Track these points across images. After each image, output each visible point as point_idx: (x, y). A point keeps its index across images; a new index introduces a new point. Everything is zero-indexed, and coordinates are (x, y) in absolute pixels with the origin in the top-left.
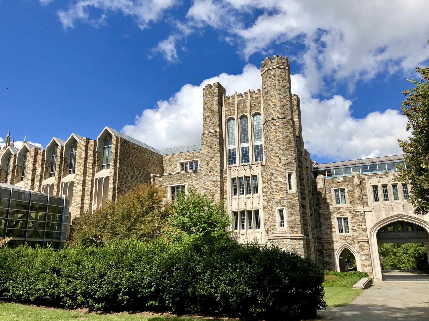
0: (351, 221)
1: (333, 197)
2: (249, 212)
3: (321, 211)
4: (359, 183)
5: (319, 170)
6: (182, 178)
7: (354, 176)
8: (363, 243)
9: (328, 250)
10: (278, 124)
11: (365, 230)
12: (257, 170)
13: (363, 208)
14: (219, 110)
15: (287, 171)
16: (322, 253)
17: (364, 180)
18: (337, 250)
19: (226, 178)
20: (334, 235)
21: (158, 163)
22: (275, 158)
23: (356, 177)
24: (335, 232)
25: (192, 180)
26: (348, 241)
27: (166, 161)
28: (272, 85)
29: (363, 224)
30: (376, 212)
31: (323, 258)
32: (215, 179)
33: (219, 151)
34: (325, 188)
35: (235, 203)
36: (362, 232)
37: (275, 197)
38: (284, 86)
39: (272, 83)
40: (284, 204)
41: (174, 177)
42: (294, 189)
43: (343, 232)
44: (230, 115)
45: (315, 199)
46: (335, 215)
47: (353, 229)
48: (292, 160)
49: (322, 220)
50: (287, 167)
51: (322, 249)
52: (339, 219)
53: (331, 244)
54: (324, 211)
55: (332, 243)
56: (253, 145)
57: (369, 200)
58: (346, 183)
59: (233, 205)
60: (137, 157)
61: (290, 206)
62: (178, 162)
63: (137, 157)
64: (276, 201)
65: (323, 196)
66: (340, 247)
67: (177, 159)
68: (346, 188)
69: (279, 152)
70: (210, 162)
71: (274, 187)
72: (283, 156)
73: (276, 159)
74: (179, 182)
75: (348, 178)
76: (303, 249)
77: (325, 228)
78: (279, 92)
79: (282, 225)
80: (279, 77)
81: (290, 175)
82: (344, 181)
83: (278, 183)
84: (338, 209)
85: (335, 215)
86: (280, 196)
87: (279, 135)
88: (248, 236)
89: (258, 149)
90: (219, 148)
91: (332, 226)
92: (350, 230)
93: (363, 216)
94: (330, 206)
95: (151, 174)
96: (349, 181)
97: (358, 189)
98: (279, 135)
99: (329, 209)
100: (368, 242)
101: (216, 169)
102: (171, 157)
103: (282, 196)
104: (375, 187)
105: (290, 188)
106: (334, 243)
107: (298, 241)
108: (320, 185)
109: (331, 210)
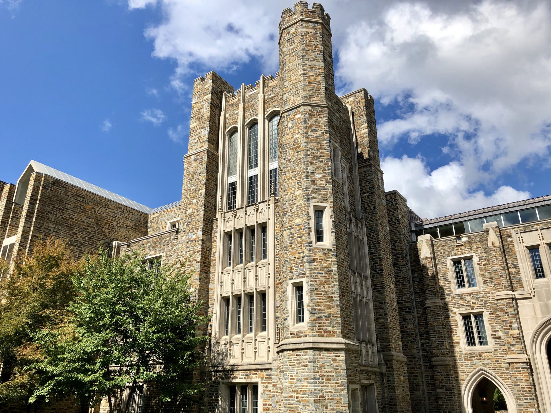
0: (489, 320)
1: (451, 275)
2: (250, 296)
4: (498, 243)
5: (425, 227)
6: (158, 244)
7: (487, 231)
8: (517, 366)
9: (444, 381)
10: (297, 116)
11: (520, 338)
12: (266, 213)
13: (511, 292)
15: (313, 203)
16: (434, 386)
17: (510, 236)
18: (465, 382)
19: (216, 235)
20: (457, 349)
22: (290, 181)
23: (491, 232)
24: (458, 343)
25: (172, 246)
26: (487, 361)
27: (151, 222)
28: (291, 51)
29: (515, 325)
30: (540, 300)
31: (437, 398)
32: (194, 237)
33: (206, 184)
35: (227, 281)
36: (514, 342)
37: (289, 257)
38: (314, 51)
39: (291, 48)
40: (304, 271)
41: (146, 244)
42: (329, 240)
43: (475, 345)
44: (231, 125)
46: (456, 310)
47: (494, 337)
48: (323, 183)
49: (431, 319)
50: (313, 195)
51: (433, 379)
52: (466, 317)
53: (451, 369)
54: (433, 301)
55: (455, 367)
56: (267, 169)
57: (522, 275)
58: (475, 246)
59: (224, 284)
60: (84, 211)
61: (318, 275)
63: (84, 211)
64: (290, 265)
65: (430, 273)
66: (471, 375)
67: (168, 217)
68: (474, 254)
69: (297, 169)
70: (189, 206)
71: (286, 239)
72: (304, 174)
74: (153, 252)
75: (478, 236)
76: (344, 373)
77: (437, 335)
78: (301, 60)
79: (301, 319)
80: (303, 36)
81: (319, 212)
82: (470, 243)
83: (295, 229)
84: (462, 297)
85: (456, 310)
86: (298, 256)
87: (298, 136)
88: (246, 346)
89: (274, 175)
90: (204, 179)
91: (451, 332)
92: (489, 339)
93: (512, 309)
94: (446, 292)
96: (480, 242)
97: (497, 254)
98: (298, 136)
100: (529, 364)
101: (197, 217)
103: (301, 255)
104: (534, 249)
105: (319, 237)
106: (459, 365)
108: (425, 252)
109: (448, 299)
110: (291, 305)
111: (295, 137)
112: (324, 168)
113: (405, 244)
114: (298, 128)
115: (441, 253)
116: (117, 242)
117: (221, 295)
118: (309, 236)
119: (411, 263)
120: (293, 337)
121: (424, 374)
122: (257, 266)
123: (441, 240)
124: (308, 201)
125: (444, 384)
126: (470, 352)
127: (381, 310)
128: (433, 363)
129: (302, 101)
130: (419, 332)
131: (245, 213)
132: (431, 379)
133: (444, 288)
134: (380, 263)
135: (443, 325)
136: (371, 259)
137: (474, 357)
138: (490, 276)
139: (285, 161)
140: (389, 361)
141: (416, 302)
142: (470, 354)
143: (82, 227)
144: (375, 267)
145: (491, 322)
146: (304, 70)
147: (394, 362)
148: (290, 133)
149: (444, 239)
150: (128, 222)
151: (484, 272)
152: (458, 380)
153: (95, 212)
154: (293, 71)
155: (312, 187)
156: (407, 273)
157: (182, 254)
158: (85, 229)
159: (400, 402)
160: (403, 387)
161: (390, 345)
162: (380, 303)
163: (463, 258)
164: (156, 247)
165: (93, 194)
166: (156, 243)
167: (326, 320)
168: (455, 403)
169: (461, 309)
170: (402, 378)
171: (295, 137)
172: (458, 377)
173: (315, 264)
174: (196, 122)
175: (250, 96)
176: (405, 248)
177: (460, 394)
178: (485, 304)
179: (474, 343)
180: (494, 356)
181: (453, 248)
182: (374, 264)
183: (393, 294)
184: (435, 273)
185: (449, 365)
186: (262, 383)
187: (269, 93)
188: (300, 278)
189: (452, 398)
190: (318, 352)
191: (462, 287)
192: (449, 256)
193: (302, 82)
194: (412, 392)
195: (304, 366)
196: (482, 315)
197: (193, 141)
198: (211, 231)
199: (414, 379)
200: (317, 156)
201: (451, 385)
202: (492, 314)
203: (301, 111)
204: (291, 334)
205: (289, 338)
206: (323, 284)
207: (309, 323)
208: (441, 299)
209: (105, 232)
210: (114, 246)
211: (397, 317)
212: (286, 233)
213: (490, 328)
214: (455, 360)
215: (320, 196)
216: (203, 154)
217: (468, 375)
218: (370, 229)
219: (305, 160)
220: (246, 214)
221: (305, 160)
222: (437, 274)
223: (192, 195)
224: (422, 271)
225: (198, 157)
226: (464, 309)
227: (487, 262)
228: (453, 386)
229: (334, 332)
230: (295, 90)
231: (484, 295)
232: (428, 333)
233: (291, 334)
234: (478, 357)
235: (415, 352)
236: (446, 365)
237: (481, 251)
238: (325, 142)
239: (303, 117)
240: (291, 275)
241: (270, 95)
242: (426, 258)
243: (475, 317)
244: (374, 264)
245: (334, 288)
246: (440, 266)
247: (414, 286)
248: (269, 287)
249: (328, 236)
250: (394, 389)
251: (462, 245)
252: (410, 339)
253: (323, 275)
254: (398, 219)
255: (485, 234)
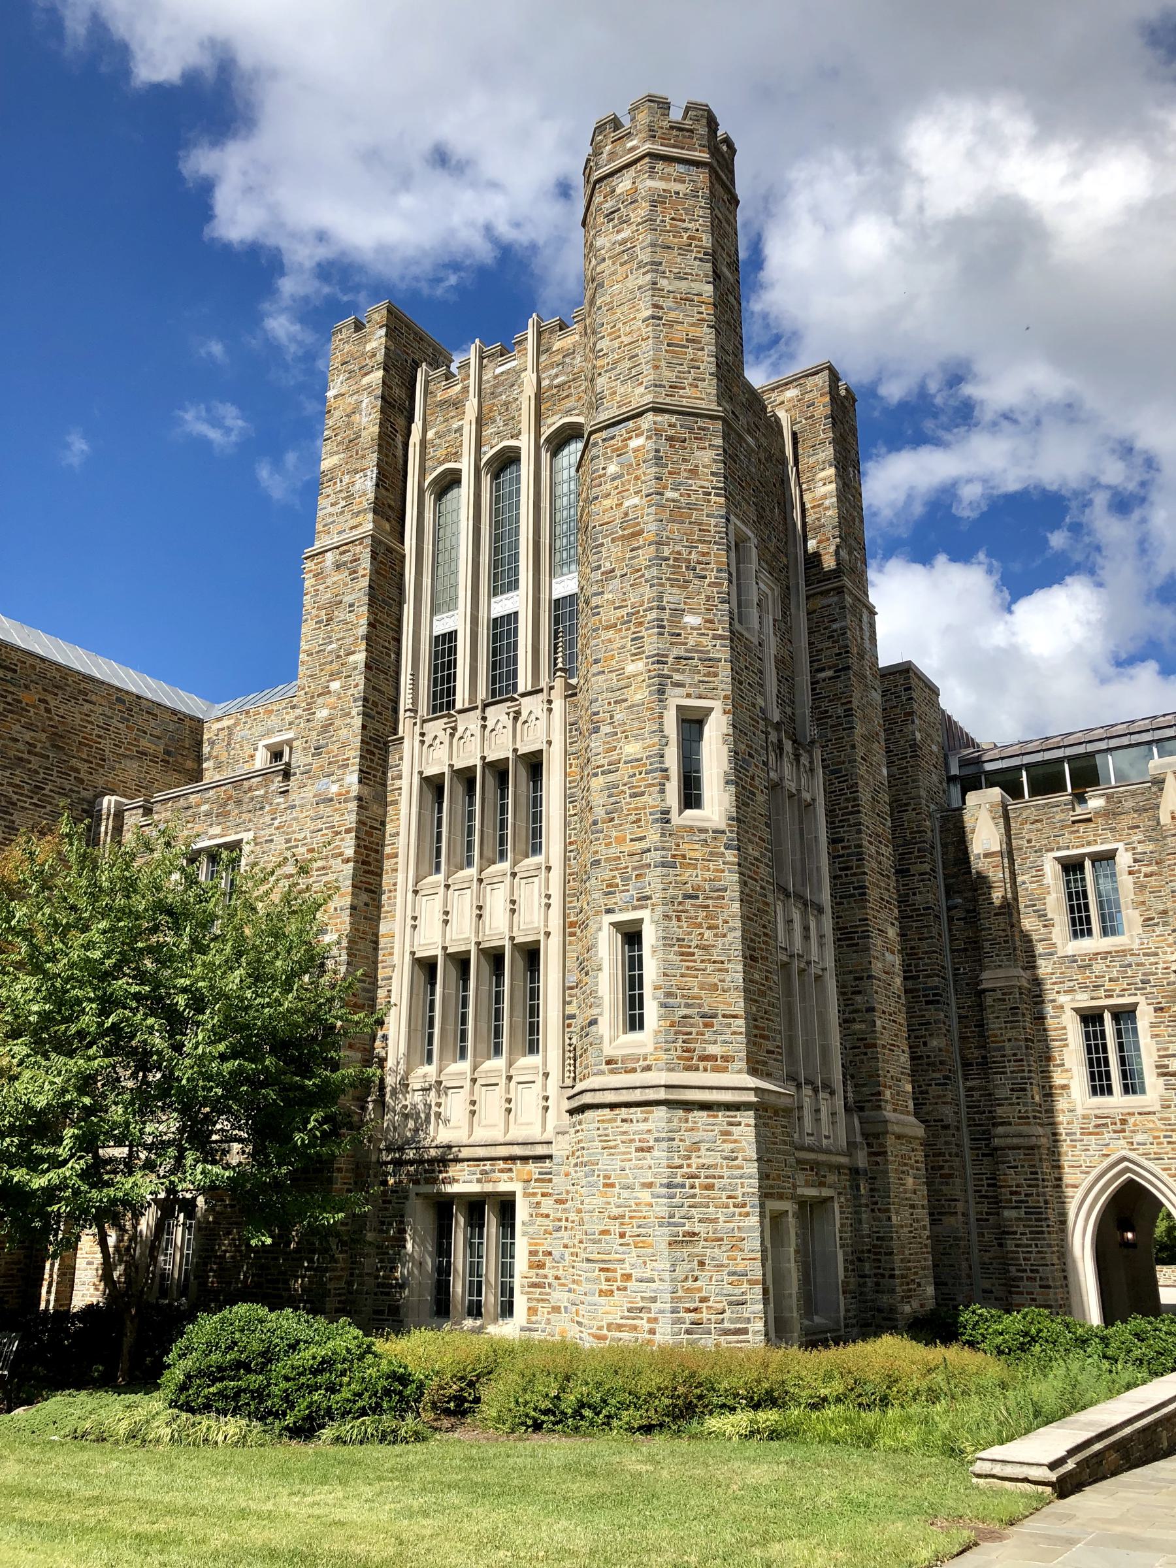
0: (1153, 1025)
2: (495, 958)
3: (990, 978)
5: (989, 767)
6: (231, 806)
9: (1024, 1190)
10: (635, 443)
12: (541, 725)
14: (383, 436)
15: (676, 699)
16: (996, 1204)
18: (1079, 1194)
19: (397, 783)
20: (1062, 1104)
21: (167, 753)
22: (610, 634)
24: (1065, 1087)
26: (1139, 1137)
27: (212, 743)
28: (619, 249)
31: (1003, 1233)
32: (335, 788)
33: (368, 638)
34: (1009, 853)
35: (430, 917)
37: (604, 852)
38: (685, 249)
39: (620, 237)
40: (647, 891)
41: (198, 806)
43: (1110, 1092)
44: (441, 464)
45: (958, 913)
46: (1063, 999)
47: (1164, 1072)
48: (704, 641)
49: (994, 1024)
50: (677, 677)
52: (1090, 1018)
53: (1043, 1157)
54: (1001, 973)
55: (1054, 1152)
56: (545, 597)
58: (1123, 822)
61: (685, 902)
62: (261, 744)
64: (607, 874)
65: (997, 896)
67: (258, 730)
68: (1120, 846)
69: (633, 598)
70: (320, 701)
71: (598, 799)
72: (653, 615)
73: (619, 639)
74: (217, 830)
75: (1133, 794)
76: (752, 1169)
77: (1010, 1066)
79: (635, 1022)
81: (692, 725)
83: (624, 772)
84: (1083, 963)
85: (1063, 999)
86: (629, 847)
87: (636, 500)
88: (480, 1093)
89: (564, 614)
90: (364, 621)
91: (1049, 1059)
94: (1040, 949)
95: (106, 798)
96: (1139, 810)
98: (636, 500)
99: (1031, 966)
101: (344, 732)
102: (235, 725)
103: (640, 845)
105: (691, 797)
106: (1065, 1147)
107: (721, 1117)
108: (984, 836)
109: (1044, 968)
110: (608, 983)
111: (627, 504)
112: (708, 598)
113: (930, 816)
114: (637, 478)
115: (1029, 841)
116: (114, 798)
117: (413, 953)
118: (662, 791)
119: (944, 868)
120: (612, 1072)
121: (969, 1171)
122: (514, 875)
123: (1030, 805)
124: (661, 692)
125: (1023, 1197)
126: (1098, 1112)
127: (858, 998)
128: (997, 1142)
129: (649, 398)
130: (962, 1058)
131: (480, 722)
132: (989, 1185)
133: (1034, 937)
134: (858, 867)
135: (1027, 1040)
136: (833, 857)
137: (1105, 1125)
138: (1161, 908)
139: (597, 576)
140: (877, 1136)
141: (955, 975)
142: (1097, 1117)
143: (11, 754)
144: (844, 880)
145: (1156, 1031)
146: (655, 306)
147: (890, 1140)
148: (614, 493)
149: (1040, 801)
150: (144, 743)
151: (1146, 896)
152: (1059, 1186)
153: (48, 711)
154: (625, 308)
155: (675, 652)
156: (933, 895)
157: (301, 836)
158: (21, 759)
159: (903, 1247)
160: (913, 1207)
161: (879, 1094)
162: (856, 979)
163: (1089, 855)
164: (226, 814)
165: (43, 659)
166: (224, 805)
167: (706, 1025)
168: (1050, 1246)
169: (1079, 996)
170: (910, 1181)
171: (627, 504)
172: (1060, 1179)
173: (678, 871)
174: (337, 453)
175: (496, 377)
176: (931, 828)
177: (1064, 1222)
178: (1143, 982)
179: (1110, 1087)
180: (1159, 1124)
181: (1063, 828)
182: (841, 869)
183: (893, 953)
184: (1009, 896)
185: (1039, 1147)
186: (526, 1195)
187: (554, 371)
188: (635, 908)
189: (1042, 1232)
190: (681, 1113)
191: (1083, 935)
192: (1052, 850)
193: (650, 341)
194: (936, 1217)
195: (641, 1150)
196: (1134, 1011)
197: (330, 510)
198: (385, 773)
199: (942, 1184)
200: (689, 561)
201: (1041, 1199)
202: (1161, 1009)
203: (645, 427)
204: (608, 1063)
205: (601, 1073)
206: (700, 926)
207: (657, 1033)
208: (1025, 969)
209: (77, 771)
210: (105, 811)
211: (902, 1018)
212: (597, 783)
213: (1154, 1047)
214: (1055, 1134)
215: (697, 678)
216: (358, 549)
217: (1088, 1173)
218: (833, 772)
219: (654, 571)
220: (484, 727)
221: (654, 571)
222: (1016, 899)
223: (328, 667)
224: (976, 890)
225: (347, 557)
226: (1085, 996)
227: (1154, 868)
228: (1046, 1202)
229: (725, 1059)
230: (628, 364)
231: (1143, 959)
232: (985, 1063)
233: (608, 1063)
234: (1118, 1127)
235: (947, 1111)
236: (1032, 1148)
237: (1141, 837)
238: (713, 521)
239: (650, 445)
240: (610, 901)
241: (557, 376)
242: (987, 855)
243: (1116, 1017)
244: (841, 869)
245: (729, 938)
246: (1026, 878)
247: (950, 930)
248: (548, 934)
249: (715, 792)
250: (888, 1210)
251: (1089, 820)
252: (938, 1075)
253: (699, 902)
254: (914, 745)
255: (1154, 789)
